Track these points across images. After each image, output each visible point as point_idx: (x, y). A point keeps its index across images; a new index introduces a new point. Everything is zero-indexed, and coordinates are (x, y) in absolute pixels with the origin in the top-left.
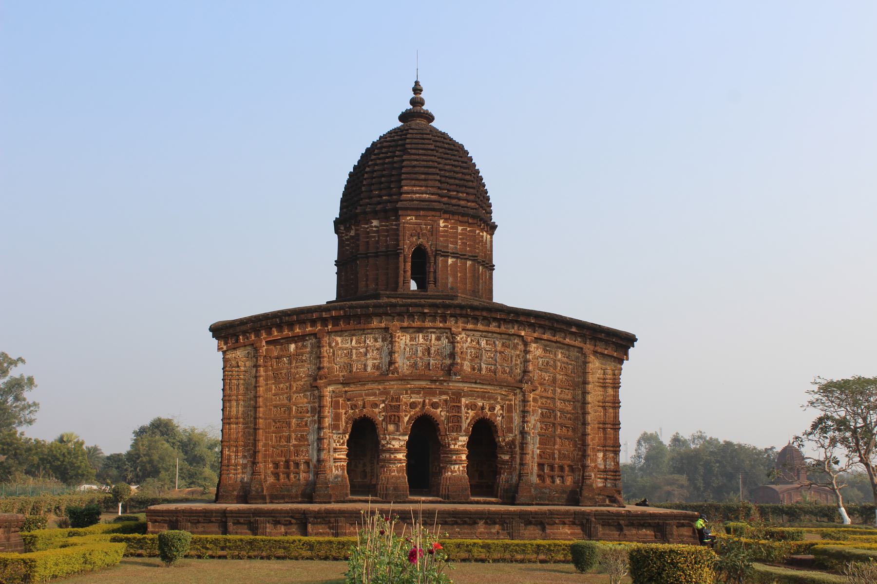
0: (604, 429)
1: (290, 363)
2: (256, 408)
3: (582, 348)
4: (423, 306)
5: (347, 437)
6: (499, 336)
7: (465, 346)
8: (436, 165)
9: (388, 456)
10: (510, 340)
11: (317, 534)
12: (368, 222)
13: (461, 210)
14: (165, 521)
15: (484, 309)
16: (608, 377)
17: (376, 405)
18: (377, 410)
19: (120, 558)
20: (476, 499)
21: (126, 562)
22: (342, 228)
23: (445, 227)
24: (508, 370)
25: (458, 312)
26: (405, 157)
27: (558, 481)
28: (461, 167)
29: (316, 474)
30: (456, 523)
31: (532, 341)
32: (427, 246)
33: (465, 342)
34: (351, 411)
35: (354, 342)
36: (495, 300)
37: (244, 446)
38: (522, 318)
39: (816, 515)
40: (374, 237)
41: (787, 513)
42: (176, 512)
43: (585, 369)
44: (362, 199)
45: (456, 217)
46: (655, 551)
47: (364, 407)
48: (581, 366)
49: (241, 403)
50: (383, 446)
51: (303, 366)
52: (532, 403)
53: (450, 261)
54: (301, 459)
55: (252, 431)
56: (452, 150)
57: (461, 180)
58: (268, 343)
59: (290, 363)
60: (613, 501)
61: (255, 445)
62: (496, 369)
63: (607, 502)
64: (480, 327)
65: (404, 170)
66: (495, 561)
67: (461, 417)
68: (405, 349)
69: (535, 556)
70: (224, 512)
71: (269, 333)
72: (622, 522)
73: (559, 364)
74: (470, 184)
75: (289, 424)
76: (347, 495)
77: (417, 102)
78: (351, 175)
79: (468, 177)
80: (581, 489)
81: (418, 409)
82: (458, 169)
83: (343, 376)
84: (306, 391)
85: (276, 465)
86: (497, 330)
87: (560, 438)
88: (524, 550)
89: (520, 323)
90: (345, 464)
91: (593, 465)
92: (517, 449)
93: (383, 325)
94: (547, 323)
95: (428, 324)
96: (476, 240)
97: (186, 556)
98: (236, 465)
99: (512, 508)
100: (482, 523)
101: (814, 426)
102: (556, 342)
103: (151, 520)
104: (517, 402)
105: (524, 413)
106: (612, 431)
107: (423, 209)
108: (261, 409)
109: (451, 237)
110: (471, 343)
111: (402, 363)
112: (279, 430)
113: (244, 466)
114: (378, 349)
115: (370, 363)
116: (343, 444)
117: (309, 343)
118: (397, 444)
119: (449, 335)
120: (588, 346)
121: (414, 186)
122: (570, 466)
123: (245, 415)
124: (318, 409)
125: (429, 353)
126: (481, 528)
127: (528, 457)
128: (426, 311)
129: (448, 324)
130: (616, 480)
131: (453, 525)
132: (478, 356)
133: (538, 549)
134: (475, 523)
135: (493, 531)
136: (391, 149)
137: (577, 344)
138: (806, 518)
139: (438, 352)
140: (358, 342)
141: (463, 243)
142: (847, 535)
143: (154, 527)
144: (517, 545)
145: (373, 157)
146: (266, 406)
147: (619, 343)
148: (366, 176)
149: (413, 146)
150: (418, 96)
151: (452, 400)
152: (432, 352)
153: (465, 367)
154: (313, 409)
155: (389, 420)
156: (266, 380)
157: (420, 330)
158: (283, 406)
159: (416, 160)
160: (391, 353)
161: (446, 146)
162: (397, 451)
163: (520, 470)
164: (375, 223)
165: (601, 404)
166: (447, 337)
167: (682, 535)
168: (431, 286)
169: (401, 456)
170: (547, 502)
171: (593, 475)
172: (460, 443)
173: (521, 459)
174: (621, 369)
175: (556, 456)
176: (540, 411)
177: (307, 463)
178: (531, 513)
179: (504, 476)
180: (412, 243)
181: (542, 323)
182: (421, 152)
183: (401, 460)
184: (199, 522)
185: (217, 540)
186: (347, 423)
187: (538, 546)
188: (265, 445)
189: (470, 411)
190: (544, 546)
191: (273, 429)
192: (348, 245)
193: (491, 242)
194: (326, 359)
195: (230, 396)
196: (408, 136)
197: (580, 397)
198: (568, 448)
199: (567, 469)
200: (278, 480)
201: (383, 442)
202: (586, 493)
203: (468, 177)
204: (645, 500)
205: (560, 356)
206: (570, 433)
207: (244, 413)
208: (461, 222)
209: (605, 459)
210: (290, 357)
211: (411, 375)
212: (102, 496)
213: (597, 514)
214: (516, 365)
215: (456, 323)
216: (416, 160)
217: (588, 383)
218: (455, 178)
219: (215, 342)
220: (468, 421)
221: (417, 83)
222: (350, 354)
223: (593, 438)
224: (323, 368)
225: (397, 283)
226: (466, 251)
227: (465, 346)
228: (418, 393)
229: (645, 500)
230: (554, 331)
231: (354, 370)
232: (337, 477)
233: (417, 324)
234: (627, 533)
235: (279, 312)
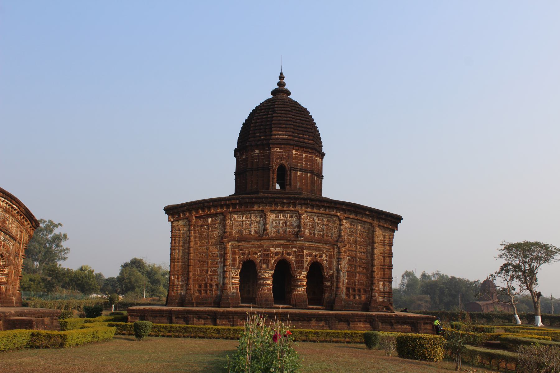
0: (384, 269)
1: (208, 229)
2: (189, 254)
4: (283, 198)
7: (306, 221)
8: (291, 119)
11: (222, 325)
12: (253, 151)
14: (138, 316)
17: (256, 254)
18: (256, 256)
19: (113, 335)
20: (311, 307)
22: (238, 154)
23: (296, 154)
25: (303, 202)
26: (274, 115)
29: (222, 291)
30: (300, 320)
31: (344, 219)
33: (306, 219)
35: (244, 218)
36: (323, 196)
37: (182, 275)
38: (338, 206)
39: (502, 318)
41: (485, 318)
42: (144, 310)
43: (373, 235)
45: (302, 149)
46: (411, 338)
47: (249, 254)
49: (181, 251)
50: (260, 276)
51: (215, 231)
52: (343, 254)
53: (299, 173)
54: (214, 282)
57: (305, 128)
59: (208, 229)
60: (388, 309)
61: (188, 274)
62: (323, 234)
64: (315, 210)
65: (273, 122)
66: (321, 341)
69: (344, 339)
70: (170, 312)
71: (197, 212)
72: (393, 321)
75: (207, 263)
76: (239, 303)
77: (281, 84)
78: (244, 124)
79: (309, 127)
80: (370, 303)
82: (304, 122)
85: (200, 286)
89: (338, 209)
90: (238, 286)
91: (377, 289)
93: (260, 208)
94: (352, 209)
96: (313, 162)
97: (149, 335)
99: (331, 312)
100: (314, 320)
101: (502, 269)
102: (357, 220)
103: (130, 315)
105: (339, 259)
107: (284, 144)
110: (309, 219)
111: (271, 230)
112: (201, 266)
113: (182, 286)
114: (257, 222)
115: (253, 230)
116: (237, 275)
117: (219, 218)
118: (268, 275)
119: (297, 214)
120: (375, 222)
121: (279, 131)
122: (364, 289)
123: (183, 258)
124: (223, 255)
126: (314, 323)
127: (341, 284)
128: (285, 201)
131: (298, 321)
132: (313, 227)
134: (311, 320)
135: (320, 325)
136: (266, 110)
137: (369, 221)
138: (496, 320)
139: (291, 224)
140: (246, 218)
142: (519, 330)
143: (131, 319)
144: (334, 333)
145: (256, 115)
147: (392, 221)
148: (252, 125)
151: (299, 251)
153: (306, 233)
154: (221, 255)
156: (195, 238)
157: (281, 212)
158: (204, 253)
160: (265, 224)
162: (267, 279)
164: (257, 151)
166: (296, 216)
167: (426, 329)
168: (288, 187)
169: (269, 282)
173: (337, 285)
176: (348, 258)
177: (217, 285)
178: (342, 315)
179: (327, 294)
180: (277, 163)
182: (283, 112)
184: (156, 317)
185: (166, 326)
186: (239, 263)
187: (346, 333)
188: (194, 275)
190: (349, 334)
191: (198, 265)
192: (241, 164)
193: (322, 163)
197: (370, 250)
198: (363, 279)
199: (362, 291)
200: (201, 294)
203: (309, 127)
204: (406, 309)
207: (182, 256)
209: (384, 285)
210: (208, 225)
212: (103, 301)
214: (335, 232)
215: (301, 208)
217: (375, 243)
219: (167, 216)
221: (281, 74)
222: (241, 225)
223: (378, 273)
225: (269, 185)
227: (306, 221)
228: (280, 247)
229: (406, 309)
230: (356, 213)
232: (233, 293)
234: (396, 327)
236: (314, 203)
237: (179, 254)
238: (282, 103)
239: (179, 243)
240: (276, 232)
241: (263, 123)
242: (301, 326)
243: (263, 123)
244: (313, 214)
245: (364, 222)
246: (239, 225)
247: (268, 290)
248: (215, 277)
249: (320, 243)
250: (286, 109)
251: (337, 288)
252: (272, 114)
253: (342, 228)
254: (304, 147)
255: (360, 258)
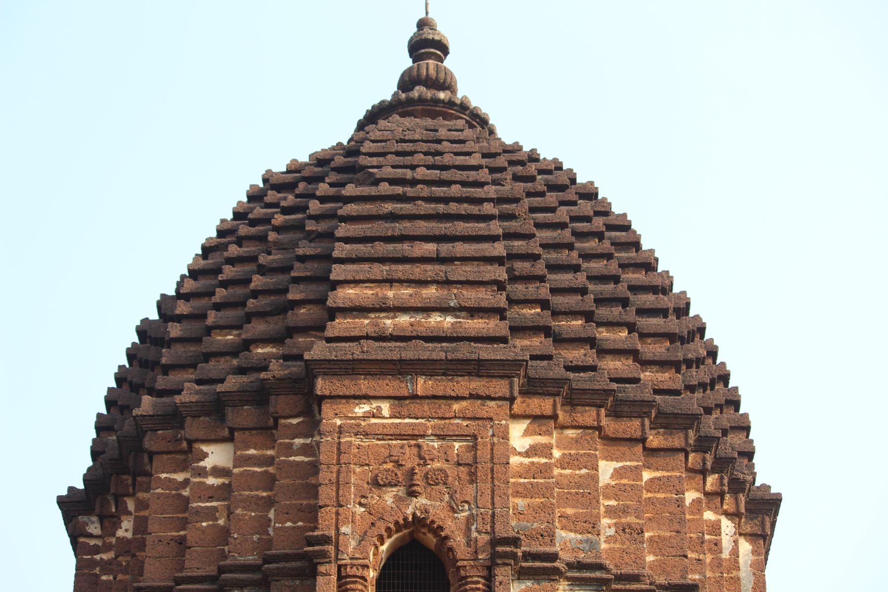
12: (186, 455)
23: (533, 451)
40: (211, 514)
45: (588, 416)
109: (566, 500)
121: (390, 282)
141: (623, 529)
164: (216, 455)
180: (375, 515)
193: (760, 567)
208: (611, 440)
226: (639, 560)
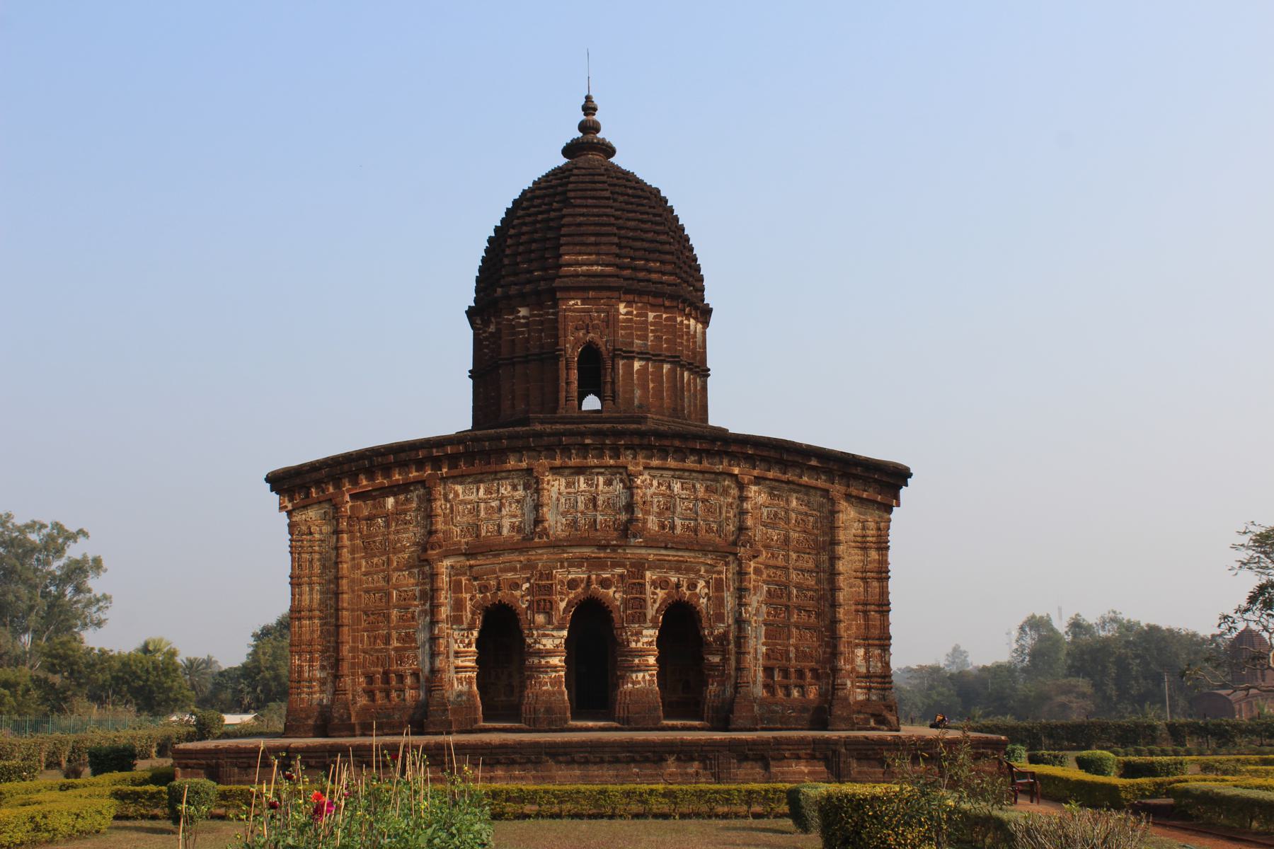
0: (865, 612)
1: (388, 525)
2: (337, 594)
3: (827, 491)
4: (583, 434)
5: (476, 634)
6: (700, 476)
7: (649, 492)
8: (612, 220)
9: (536, 661)
10: (717, 481)
13: (652, 287)
14: (200, 766)
15: (696, 437)
16: (870, 532)
17: (517, 586)
18: (518, 593)
20: (670, 723)
21: (117, 828)
22: (479, 321)
23: (627, 313)
24: (715, 526)
25: (636, 441)
26: (565, 211)
27: (795, 693)
28: (652, 223)
29: (429, 691)
30: (633, 760)
31: (750, 483)
32: (601, 343)
33: (649, 486)
34: (479, 596)
36: (714, 420)
37: (322, 652)
38: (733, 448)
39: (1259, 734)
40: (522, 333)
41: (1213, 734)
42: (217, 752)
43: (833, 521)
44: (503, 277)
45: (645, 299)
46: (851, 798)
47: (499, 589)
48: (827, 518)
50: (529, 646)
51: (406, 530)
52: (753, 576)
53: (637, 365)
54: (407, 668)
55: (332, 628)
56: (639, 197)
57: (652, 241)
58: (353, 497)
59: (388, 525)
60: (882, 721)
63: (872, 723)
64: (671, 463)
65: (564, 230)
67: (644, 600)
68: (558, 499)
69: (745, 807)
71: (355, 482)
73: (794, 515)
74: (667, 247)
76: (476, 721)
77: (588, 127)
78: (490, 240)
79: (663, 238)
80: (831, 705)
81: (580, 590)
82: (647, 226)
83: (467, 543)
84: (411, 567)
85: (370, 679)
86: (698, 467)
87: (797, 628)
88: (727, 800)
89: (733, 457)
91: (848, 667)
92: (732, 646)
93: (524, 465)
94: (772, 454)
95: (592, 461)
96: (675, 331)
98: (310, 681)
99: (718, 736)
101: (1253, 599)
102: (788, 482)
103: (179, 765)
104: (730, 576)
105: (741, 592)
106: (877, 616)
108: (345, 596)
109: (637, 329)
110: (658, 489)
111: (554, 521)
112: (372, 627)
113: (323, 682)
114: (518, 501)
115: (506, 523)
116: (469, 645)
118: (551, 642)
119: (624, 476)
121: (580, 254)
122: (812, 670)
125: (595, 506)
126: (671, 767)
127: (749, 658)
128: (588, 441)
129: (622, 460)
130: (884, 689)
131: (628, 763)
132: (669, 508)
133: (749, 797)
136: (547, 200)
137: (820, 483)
138: (1242, 741)
139: (608, 504)
140: (488, 491)
141: (656, 337)
142: (1239, 767)
144: (717, 792)
145: (521, 213)
146: (353, 591)
147: (886, 481)
148: (509, 242)
149: (579, 194)
150: (590, 118)
151: (632, 575)
152: (600, 503)
153: (650, 525)
154: (423, 593)
155: (536, 607)
156: (352, 552)
157: (580, 470)
158: (379, 590)
159: (583, 215)
160: (537, 506)
161: (630, 192)
162: (550, 653)
163: (737, 678)
164: (523, 312)
165: (859, 575)
166: (621, 481)
170: (779, 726)
171: (849, 683)
172: (645, 640)
173: (738, 661)
174: (889, 521)
175: (792, 655)
178: (746, 742)
179: (713, 688)
180: (577, 340)
181: (765, 454)
183: (555, 667)
186: (473, 613)
187: (750, 792)
188: (353, 649)
189: (658, 591)
190: (758, 793)
191: (364, 624)
192: (487, 347)
193: (704, 334)
194: (440, 519)
195: (299, 577)
196: (572, 179)
197: (827, 565)
198: (810, 642)
199: (809, 674)
201: (529, 641)
202: (838, 711)
203: (663, 238)
205: (794, 503)
206: (813, 619)
207: (321, 602)
208: (652, 305)
209: (867, 658)
210: (386, 516)
211: (567, 539)
212: (183, 731)
213: (848, 743)
214: (728, 518)
215: (635, 458)
216: (583, 215)
217: (838, 544)
218: (643, 240)
219: (275, 497)
220: (657, 605)
221: (588, 98)
223: (848, 625)
224: (436, 532)
225: (557, 401)
226: (661, 349)
227: (649, 492)
228: (580, 566)
230: (785, 466)
231: (483, 534)
232: (460, 694)
233: (575, 461)
235: (367, 450)
236: (666, 442)
237: (313, 597)
238: (587, 179)
239: (311, 566)
240: (568, 525)
241: (536, 236)
242: (637, 775)
243: (536, 236)
244: (666, 473)
245: (808, 487)
246: (470, 512)
247: (555, 682)
248: (410, 653)
249: (687, 549)
250: (598, 194)
251: (739, 669)
252: (560, 210)
253: (748, 506)
254: (648, 293)
255: (799, 587)
